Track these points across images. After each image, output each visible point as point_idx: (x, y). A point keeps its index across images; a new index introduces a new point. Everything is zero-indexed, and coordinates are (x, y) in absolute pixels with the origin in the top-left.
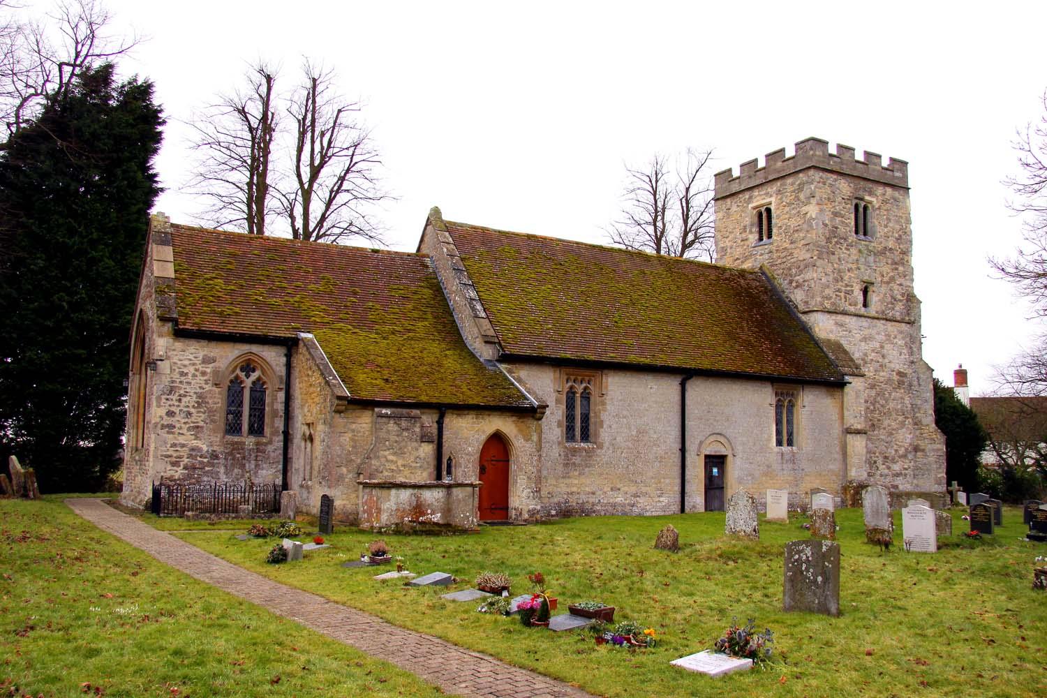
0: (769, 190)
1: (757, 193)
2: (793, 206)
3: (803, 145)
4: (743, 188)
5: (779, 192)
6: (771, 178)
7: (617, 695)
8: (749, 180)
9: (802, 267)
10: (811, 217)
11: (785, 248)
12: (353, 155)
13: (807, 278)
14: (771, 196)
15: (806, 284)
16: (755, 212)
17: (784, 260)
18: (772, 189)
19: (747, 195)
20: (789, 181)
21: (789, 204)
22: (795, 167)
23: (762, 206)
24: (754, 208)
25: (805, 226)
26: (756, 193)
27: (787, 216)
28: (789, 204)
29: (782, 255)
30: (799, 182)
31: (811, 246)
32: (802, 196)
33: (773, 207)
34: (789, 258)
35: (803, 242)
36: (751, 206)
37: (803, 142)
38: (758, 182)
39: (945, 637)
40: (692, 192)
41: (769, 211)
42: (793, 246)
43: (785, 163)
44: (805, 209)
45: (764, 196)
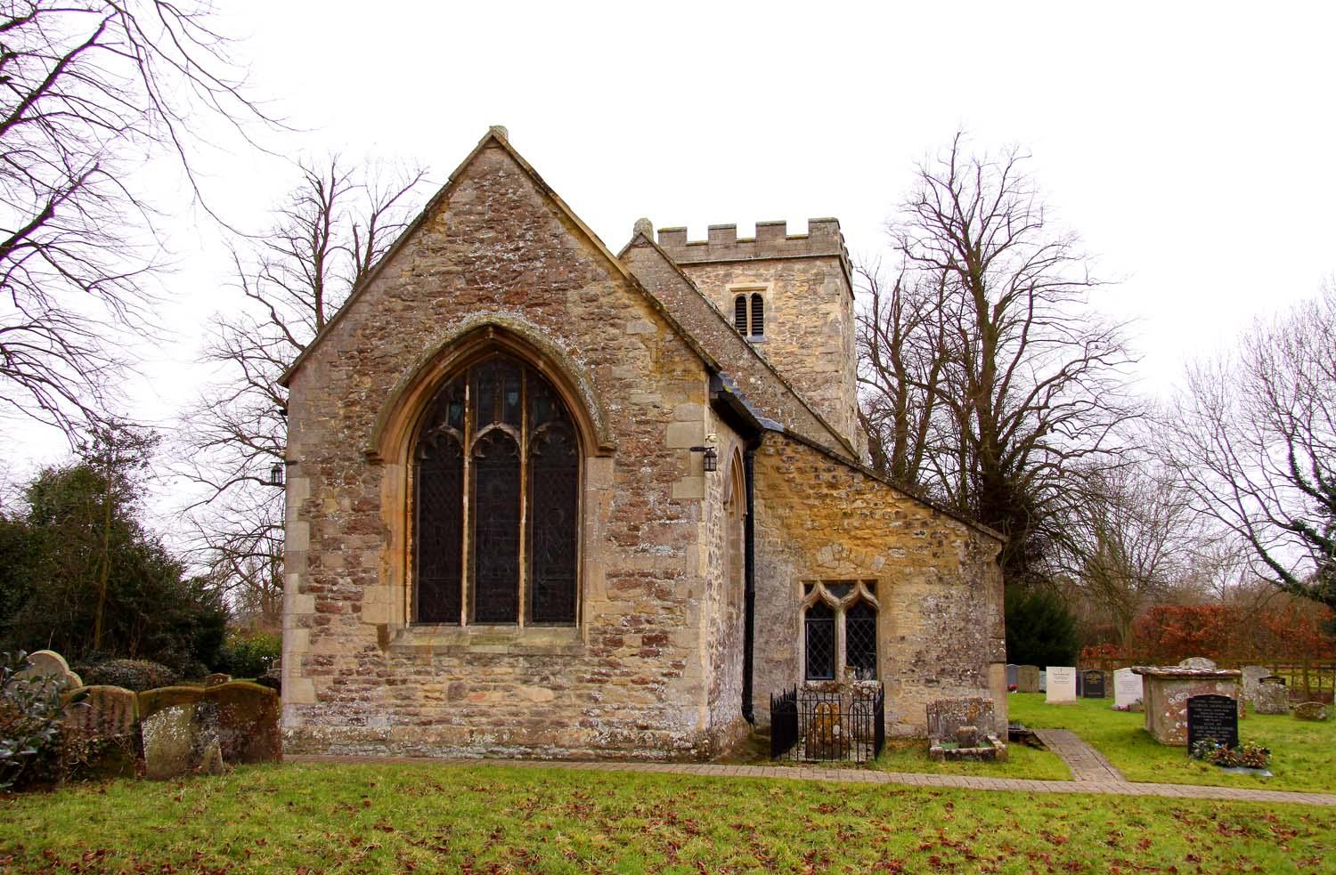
0: (762, 271)
1: (739, 272)
2: (805, 300)
3: (823, 225)
4: (712, 259)
5: (779, 277)
6: (764, 256)
7: (494, 869)
8: (726, 251)
9: (819, 381)
10: (836, 319)
11: (792, 353)
12: (1009, 223)
13: (828, 395)
14: (766, 280)
15: (827, 403)
16: (734, 296)
17: (790, 367)
18: (772, 270)
19: (721, 271)
20: (798, 266)
21: (797, 297)
22: (809, 250)
23: (749, 290)
24: (733, 291)
25: (826, 330)
26: (738, 270)
27: (794, 311)
28: (797, 297)
29: (785, 361)
30: (815, 271)
31: (835, 357)
32: (821, 289)
33: (768, 297)
34: (799, 365)
35: (821, 349)
36: (728, 286)
37: (822, 221)
38: (740, 257)
39: (1003, 794)
40: (377, 225)
41: (757, 299)
42: (804, 351)
43: (790, 242)
44: (824, 308)
45: (753, 278)
